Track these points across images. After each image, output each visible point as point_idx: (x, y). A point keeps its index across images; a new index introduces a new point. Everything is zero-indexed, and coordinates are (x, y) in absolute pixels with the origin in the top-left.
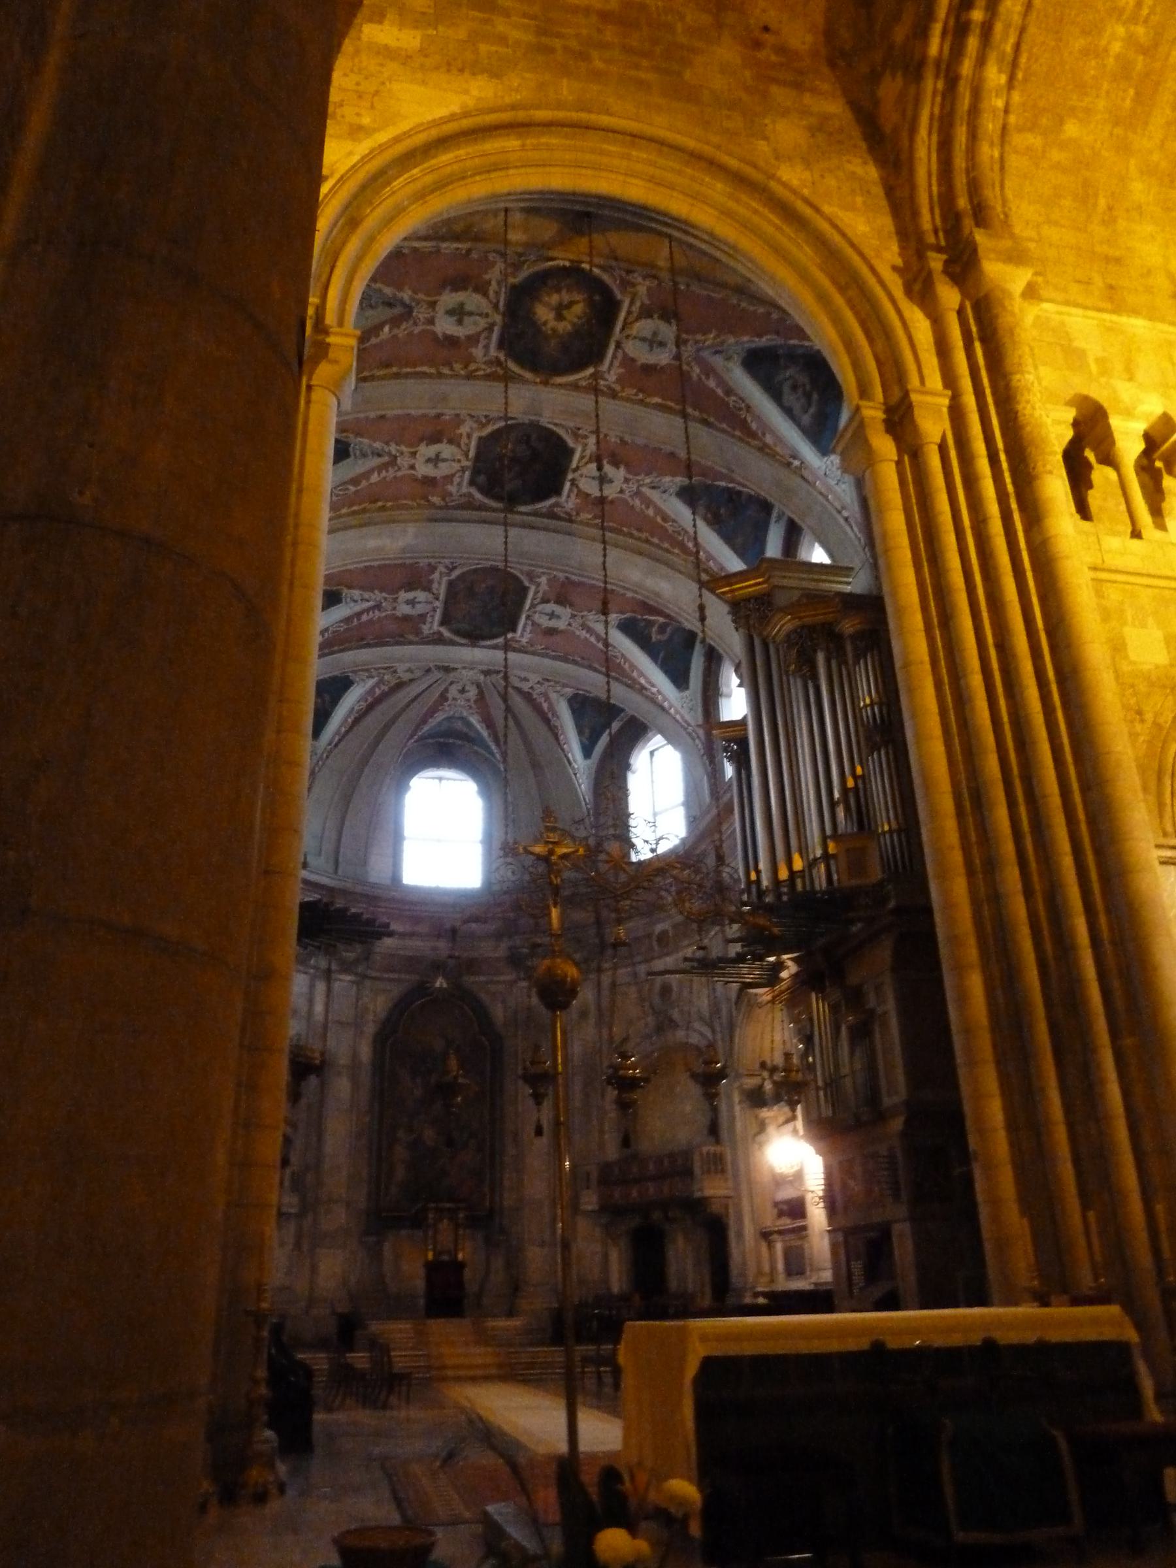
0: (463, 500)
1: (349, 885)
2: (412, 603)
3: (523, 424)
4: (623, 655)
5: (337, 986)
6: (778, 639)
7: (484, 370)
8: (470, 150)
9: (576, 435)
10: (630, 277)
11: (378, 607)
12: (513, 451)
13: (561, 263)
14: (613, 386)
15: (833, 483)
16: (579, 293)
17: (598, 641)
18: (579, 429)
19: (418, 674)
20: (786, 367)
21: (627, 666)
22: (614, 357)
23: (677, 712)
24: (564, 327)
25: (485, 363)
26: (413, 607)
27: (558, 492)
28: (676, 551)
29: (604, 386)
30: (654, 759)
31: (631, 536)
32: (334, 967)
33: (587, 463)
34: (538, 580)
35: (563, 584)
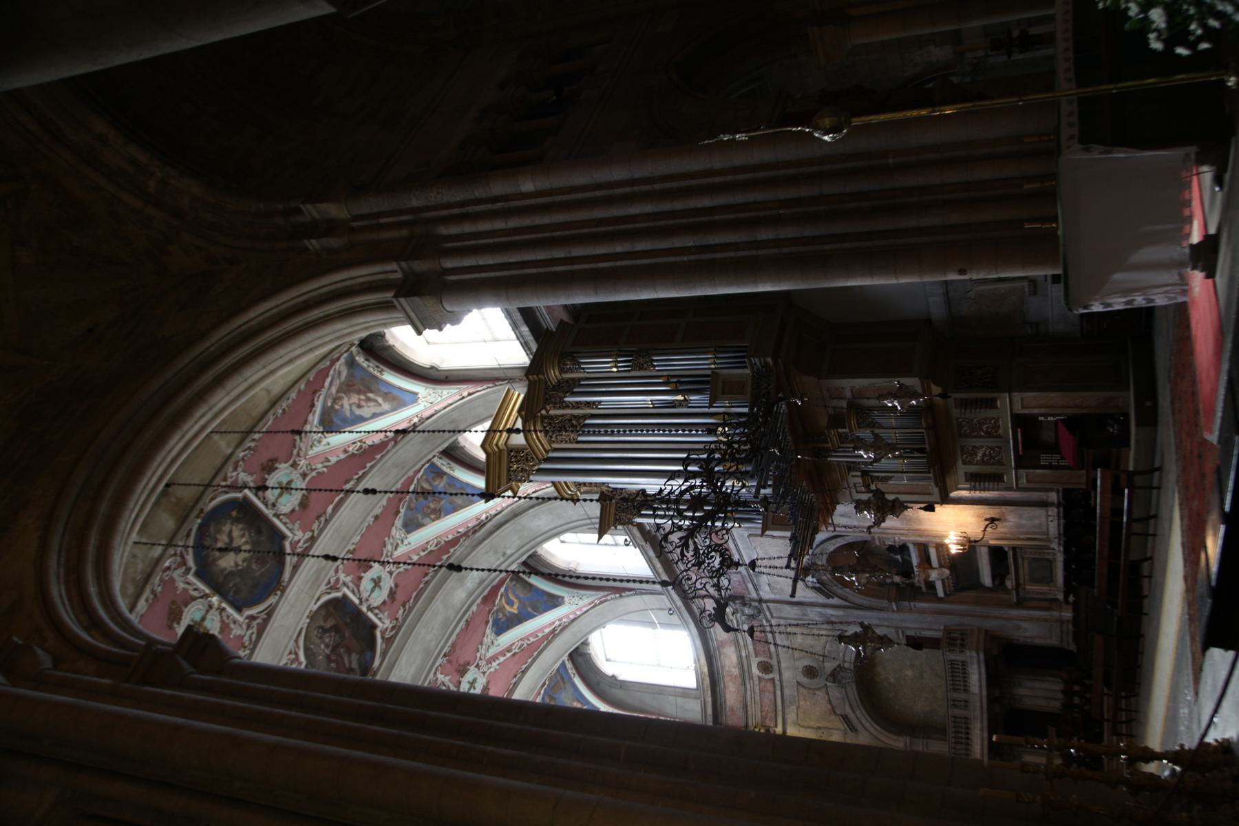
3: (309, 624)
4: (521, 639)
6: (548, 447)
7: (253, 633)
9: (334, 588)
12: (327, 646)
14: (306, 537)
15: (439, 399)
16: (224, 525)
17: (505, 655)
18: (329, 582)
20: (342, 406)
21: (532, 640)
22: (285, 524)
23: (580, 609)
27: (374, 627)
28: (452, 550)
30: (612, 659)
31: (427, 583)
33: (359, 591)
34: (439, 682)
35: (449, 661)
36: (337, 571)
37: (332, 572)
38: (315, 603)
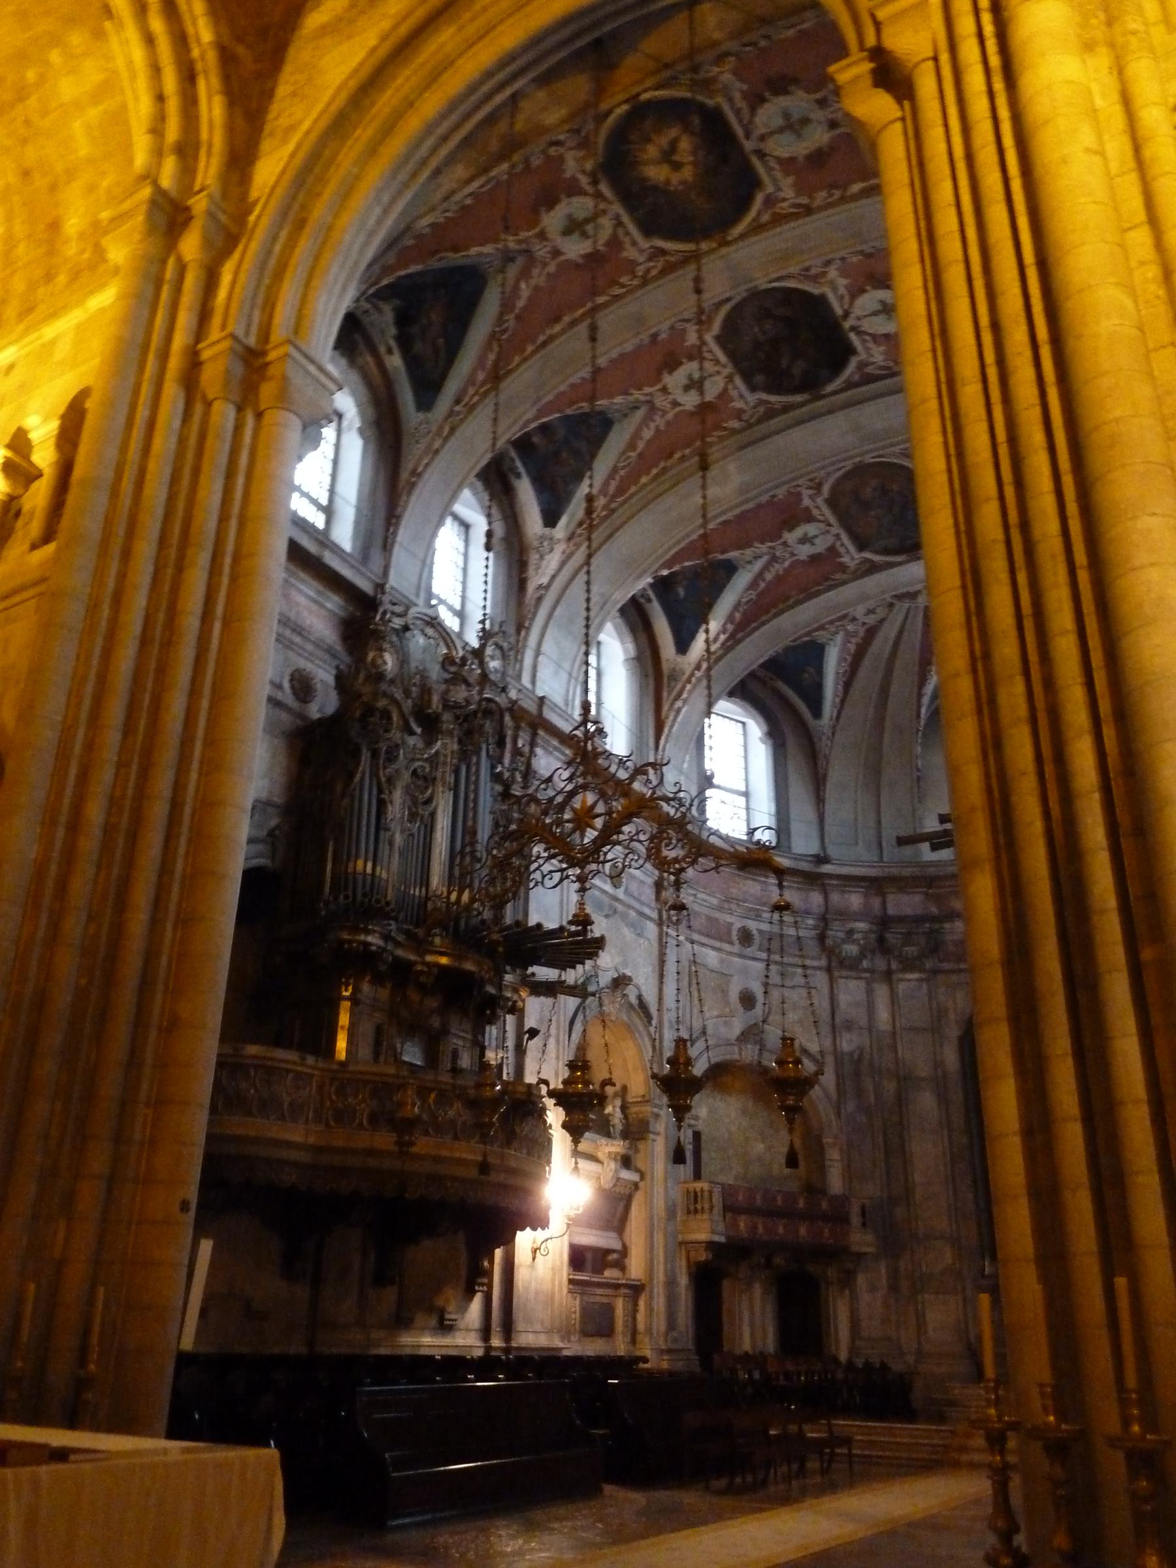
0: (761, 409)
1: (894, 871)
2: (804, 540)
5: (901, 987)
7: (653, 267)
8: (407, 72)
10: (702, 75)
11: (774, 559)
13: (619, 111)
18: (807, 269)
19: (881, 613)
24: (687, 173)
25: (650, 259)
26: (813, 544)
27: (850, 351)
29: (790, 207)
32: (894, 966)
36: (828, 263)
37: (819, 262)
38: (770, 282)
